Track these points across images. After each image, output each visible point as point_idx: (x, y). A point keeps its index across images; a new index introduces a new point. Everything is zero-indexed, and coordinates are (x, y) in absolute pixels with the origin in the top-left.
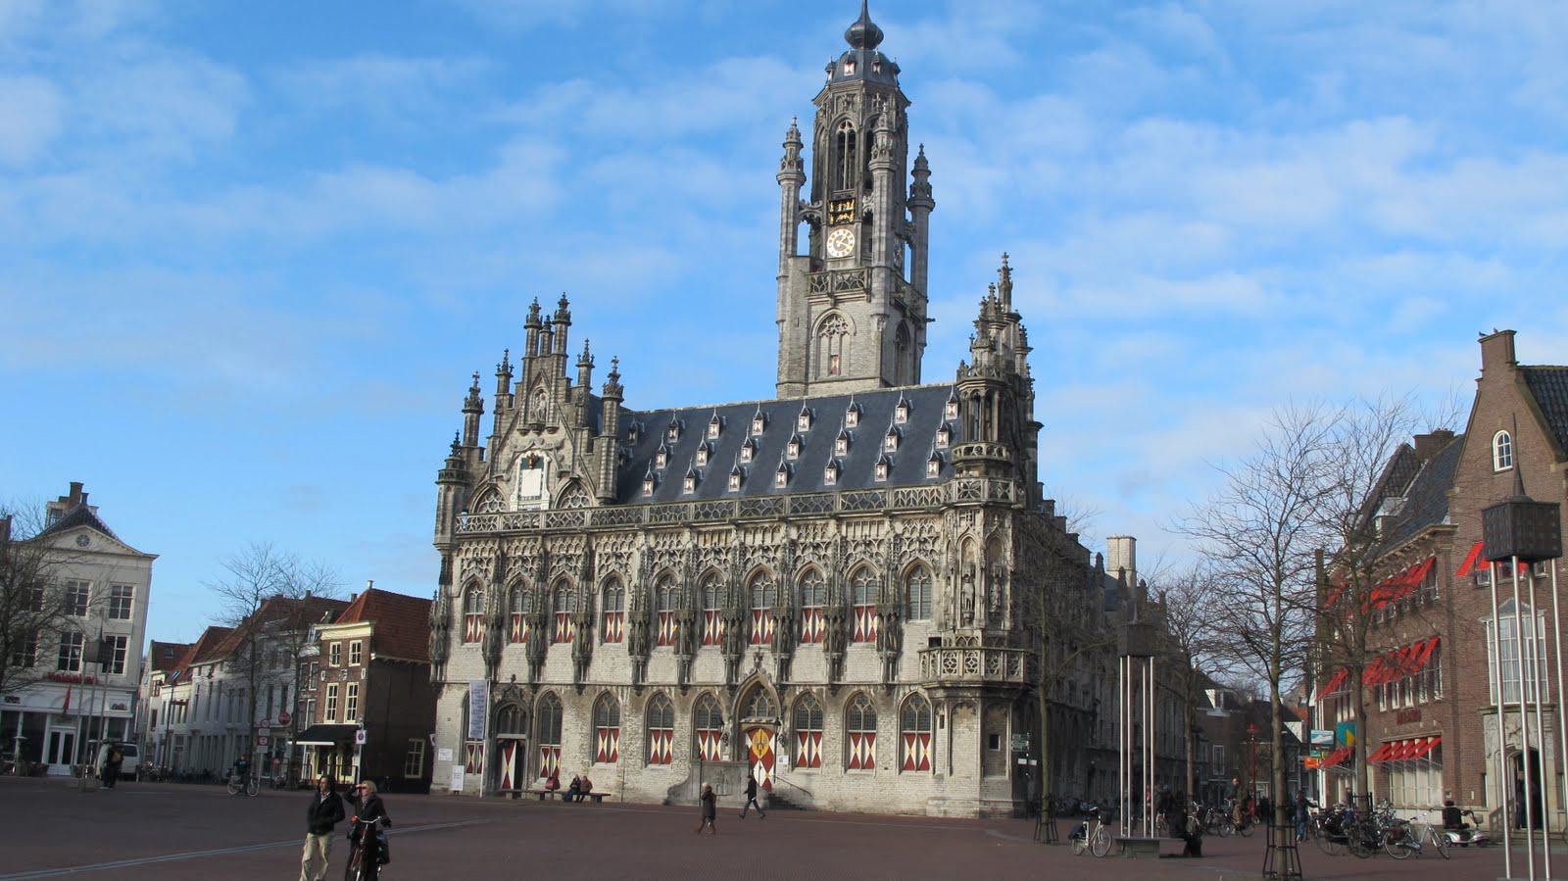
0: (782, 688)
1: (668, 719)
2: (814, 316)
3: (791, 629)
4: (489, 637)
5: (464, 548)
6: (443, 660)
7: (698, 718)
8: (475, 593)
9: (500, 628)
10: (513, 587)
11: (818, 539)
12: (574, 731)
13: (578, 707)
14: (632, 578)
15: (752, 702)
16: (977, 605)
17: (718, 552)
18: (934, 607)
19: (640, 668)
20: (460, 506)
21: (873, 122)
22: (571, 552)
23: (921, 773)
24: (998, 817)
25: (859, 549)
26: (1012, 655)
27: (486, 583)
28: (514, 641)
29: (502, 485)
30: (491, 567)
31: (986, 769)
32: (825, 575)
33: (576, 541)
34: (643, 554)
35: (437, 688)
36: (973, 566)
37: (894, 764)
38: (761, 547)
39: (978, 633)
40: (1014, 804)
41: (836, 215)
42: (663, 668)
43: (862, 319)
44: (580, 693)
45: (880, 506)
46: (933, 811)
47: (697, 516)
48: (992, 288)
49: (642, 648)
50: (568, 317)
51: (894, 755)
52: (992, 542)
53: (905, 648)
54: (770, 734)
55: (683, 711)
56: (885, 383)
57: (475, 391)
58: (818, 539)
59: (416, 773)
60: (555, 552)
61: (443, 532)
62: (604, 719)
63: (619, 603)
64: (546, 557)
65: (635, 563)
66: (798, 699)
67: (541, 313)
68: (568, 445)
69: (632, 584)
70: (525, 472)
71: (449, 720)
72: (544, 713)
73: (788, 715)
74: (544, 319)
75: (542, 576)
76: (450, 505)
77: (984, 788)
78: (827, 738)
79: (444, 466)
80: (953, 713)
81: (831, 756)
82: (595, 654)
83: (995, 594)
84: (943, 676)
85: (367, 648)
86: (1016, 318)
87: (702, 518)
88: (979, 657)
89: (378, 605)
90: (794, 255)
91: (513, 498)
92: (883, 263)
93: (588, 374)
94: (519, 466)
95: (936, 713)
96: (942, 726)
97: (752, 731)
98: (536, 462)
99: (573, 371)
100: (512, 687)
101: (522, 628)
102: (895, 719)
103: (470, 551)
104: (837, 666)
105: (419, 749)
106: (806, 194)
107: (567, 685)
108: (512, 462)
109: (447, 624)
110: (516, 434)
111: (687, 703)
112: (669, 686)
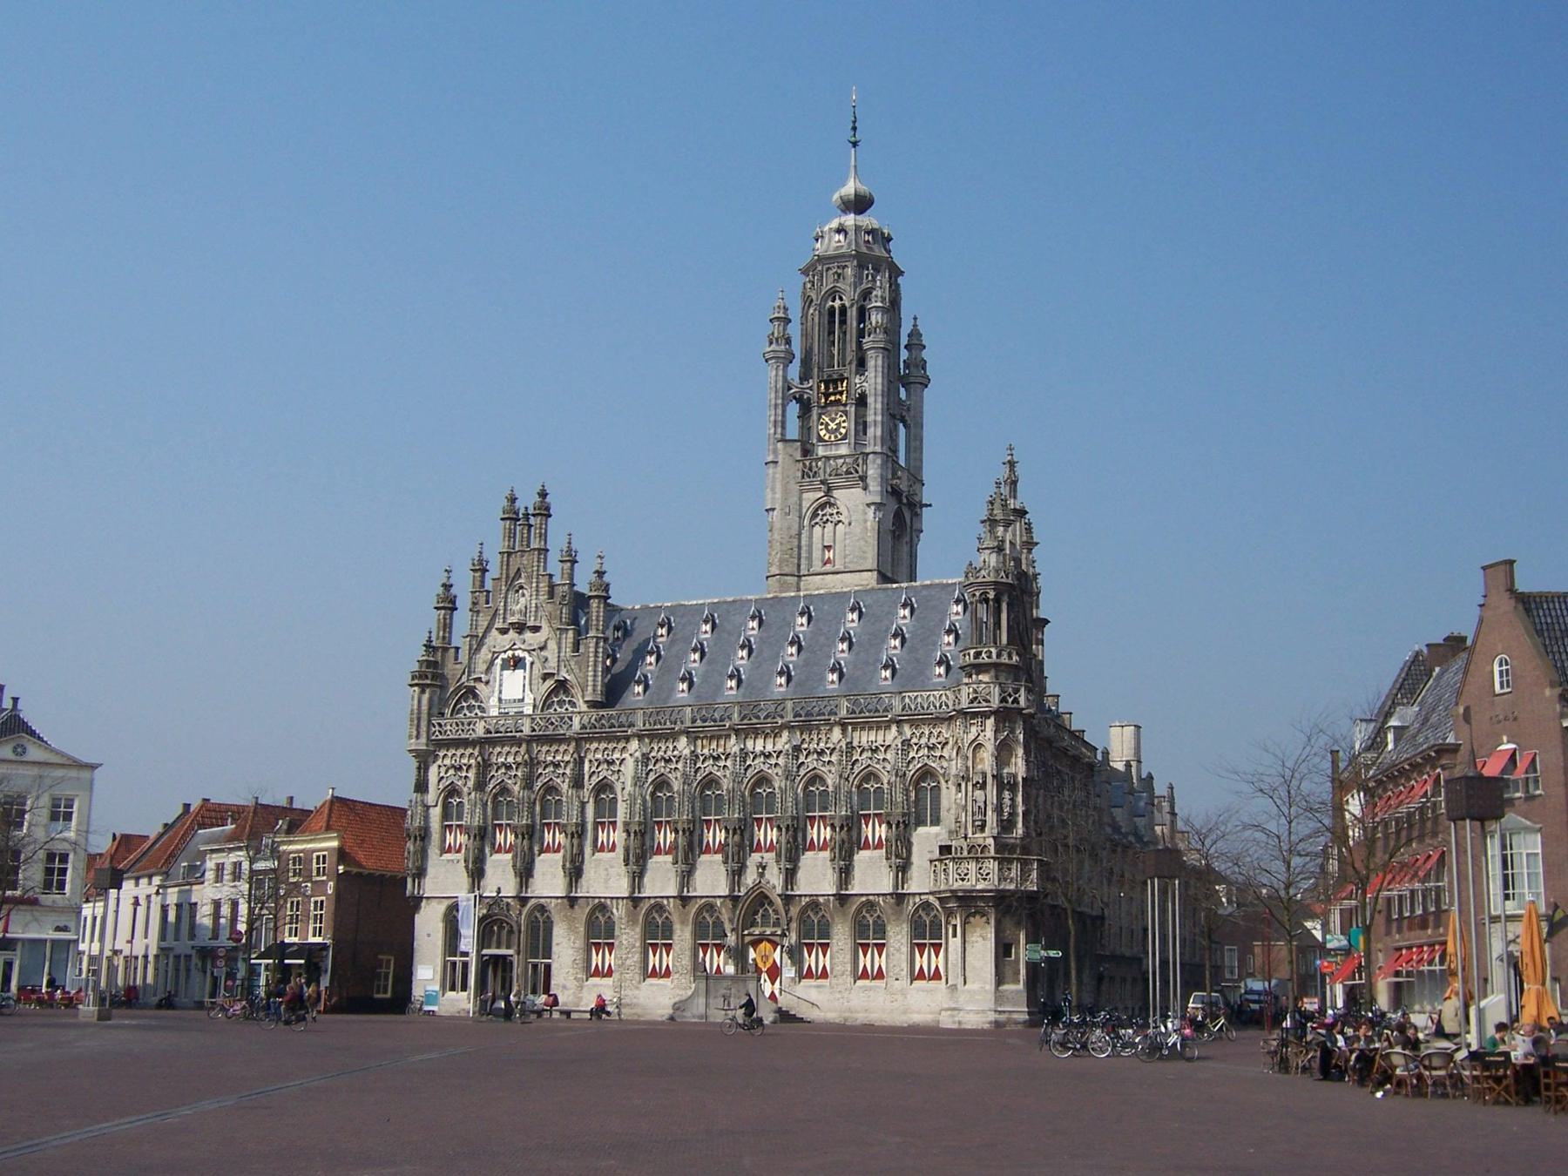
0: (788, 899)
1: (668, 931)
2: (805, 505)
3: (795, 838)
4: (471, 846)
5: (441, 754)
6: (420, 873)
7: (700, 930)
8: (455, 801)
9: (482, 838)
10: (495, 796)
11: (822, 745)
13: (571, 922)
15: (756, 913)
16: (989, 812)
17: (717, 758)
18: (943, 814)
19: (637, 877)
20: (435, 711)
21: (866, 295)
22: (559, 758)
23: (933, 983)
24: (1013, 1027)
25: (865, 755)
26: (1025, 863)
27: (465, 790)
28: (499, 851)
29: (480, 687)
30: (472, 774)
31: (1000, 979)
32: (829, 782)
33: (563, 748)
34: (637, 761)
35: (416, 903)
36: (984, 775)
37: (905, 973)
38: (763, 753)
39: (991, 841)
40: (1029, 1013)
41: (827, 395)
42: (661, 880)
43: (858, 510)
44: (572, 906)
45: (886, 710)
46: (947, 1022)
47: (694, 721)
48: (998, 484)
49: (638, 860)
50: (548, 509)
51: (905, 966)
52: (1003, 751)
53: (915, 858)
54: (775, 945)
55: (683, 922)
56: (884, 578)
58: (822, 745)
59: (385, 992)
60: (542, 758)
61: (418, 737)
62: (599, 930)
63: (613, 813)
64: (532, 763)
65: (629, 769)
66: (804, 911)
67: (517, 504)
68: (552, 645)
69: (626, 792)
72: (533, 926)
73: (794, 925)
74: (522, 511)
75: (528, 784)
76: (425, 708)
77: (999, 997)
78: (835, 948)
79: (416, 667)
80: (965, 923)
81: (838, 968)
82: (586, 867)
83: (1007, 801)
84: (956, 886)
85: (335, 859)
86: (1021, 513)
87: (699, 723)
88: (992, 866)
89: (343, 811)
90: (783, 440)
91: (494, 701)
92: (878, 449)
93: (572, 569)
95: (947, 923)
96: (955, 935)
97: (755, 944)
98: (517, 663)
99: (555, 566)
100: (497, 900)
101: (505, 838)
102: (905, 928)
103: (448, 757)
104: (845, 874)
105: (388, 967)
106: (794, 370)
108: (492, 663)
109: (424, 835)
110: (494, 633)
111: (687, 914)
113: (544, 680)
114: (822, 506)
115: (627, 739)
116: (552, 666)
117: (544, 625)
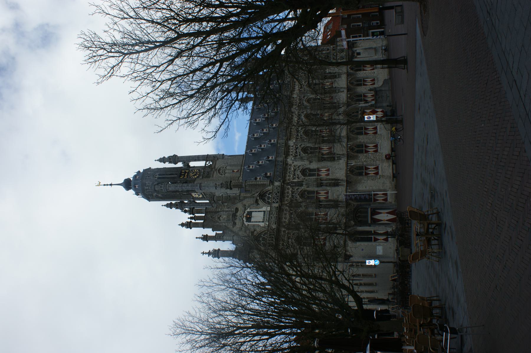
1: (360, 146)
12: (365, 186)
14: (305, 164)
44: (350, 182)
55: (357, 138)
57: (209, 253)
65: (298, 163)
70: (252, 220)
71: (363, 250)
94: (249, 223)
95: (356, 57)
96: (359, 54)
98: (250, 213)
107: (347, 189)
108: (247, 228)
112: (347, 145)
113: (258, 204)
114: (219, 172)
115: (287, 164)
116: (252, 201)
117: (236, 206)
